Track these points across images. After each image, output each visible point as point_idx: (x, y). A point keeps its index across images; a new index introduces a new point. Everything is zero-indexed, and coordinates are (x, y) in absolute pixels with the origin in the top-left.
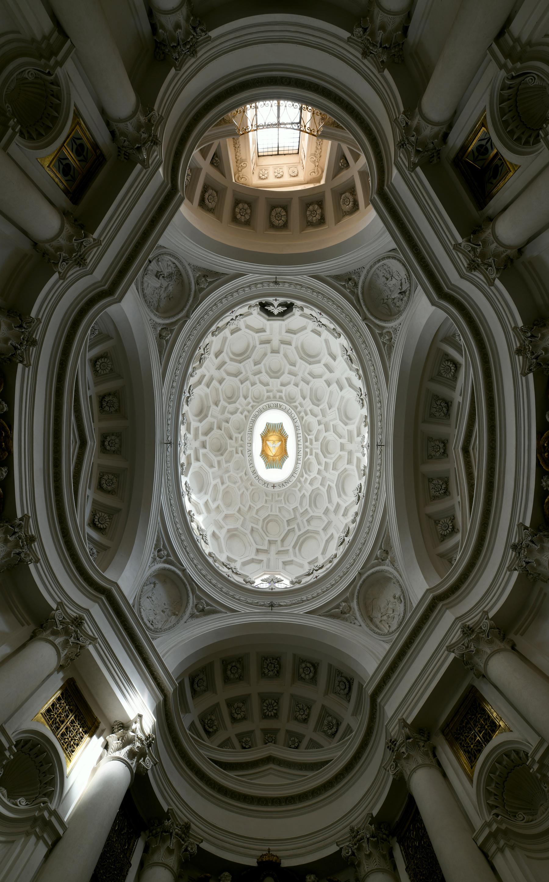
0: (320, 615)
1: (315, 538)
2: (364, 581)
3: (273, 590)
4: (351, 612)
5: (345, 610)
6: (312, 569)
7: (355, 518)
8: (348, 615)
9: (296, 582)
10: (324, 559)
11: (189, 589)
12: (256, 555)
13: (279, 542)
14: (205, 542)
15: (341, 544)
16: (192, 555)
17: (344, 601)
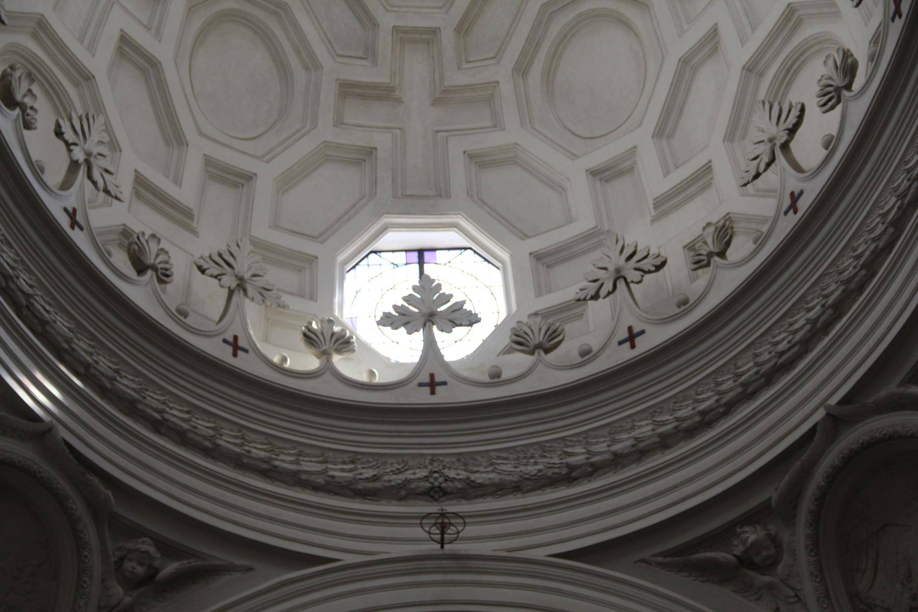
0: (643, 561)
1: (624, 23)
2: (850, 459)
3: (443, 397)
4: (780, 568)
5: (757, 560)
6: (612, 268)
7: (838, 90)
8: (767, 579)
9: (539, 346)
10: (666, 173)
11: (79, 508)
12: (339, 122)
13: (447, 37)
14: (107, 191)
15: (757, 176)
16: (62, 324)
17: (751, 519)
